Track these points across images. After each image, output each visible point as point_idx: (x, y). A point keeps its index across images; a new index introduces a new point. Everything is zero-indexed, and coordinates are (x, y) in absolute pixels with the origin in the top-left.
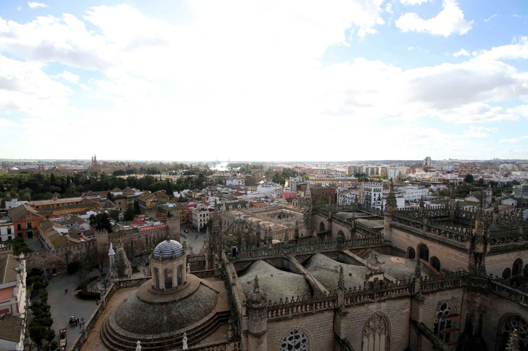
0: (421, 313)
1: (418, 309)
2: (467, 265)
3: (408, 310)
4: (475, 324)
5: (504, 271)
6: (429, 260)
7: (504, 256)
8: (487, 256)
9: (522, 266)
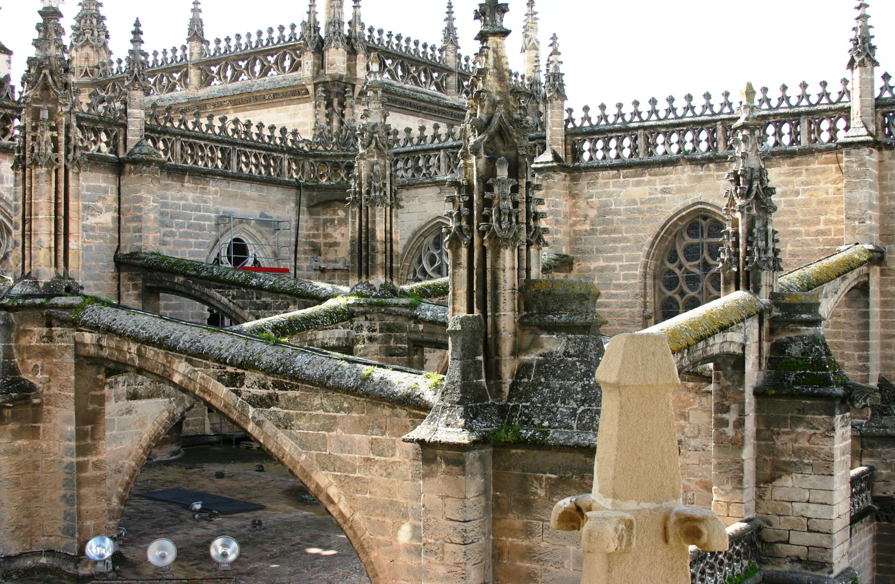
0: (152, 216)
1: (140, 199)
3: (107, 218)
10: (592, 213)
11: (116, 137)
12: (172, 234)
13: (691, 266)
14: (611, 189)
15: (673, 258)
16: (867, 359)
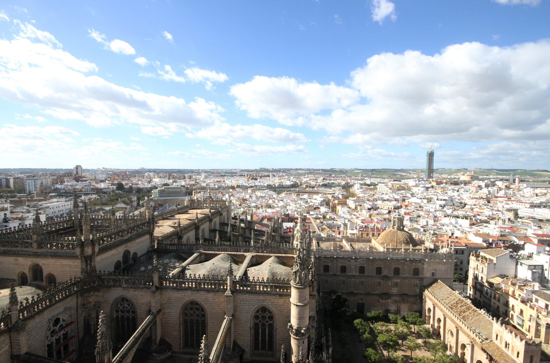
1: (19, 340)
2: (80, 270)
4: (93, 322)
5: (116, 264)
6: (44, 279)
7: (114, 252)
8: (97, 256)
9: (130, 256)
10: (166, 299)
11: (7, 321)
12: (32, 335)
13: (191, 312)
14: (171, 294)
15: (187, 310)
16: (231, 340)
